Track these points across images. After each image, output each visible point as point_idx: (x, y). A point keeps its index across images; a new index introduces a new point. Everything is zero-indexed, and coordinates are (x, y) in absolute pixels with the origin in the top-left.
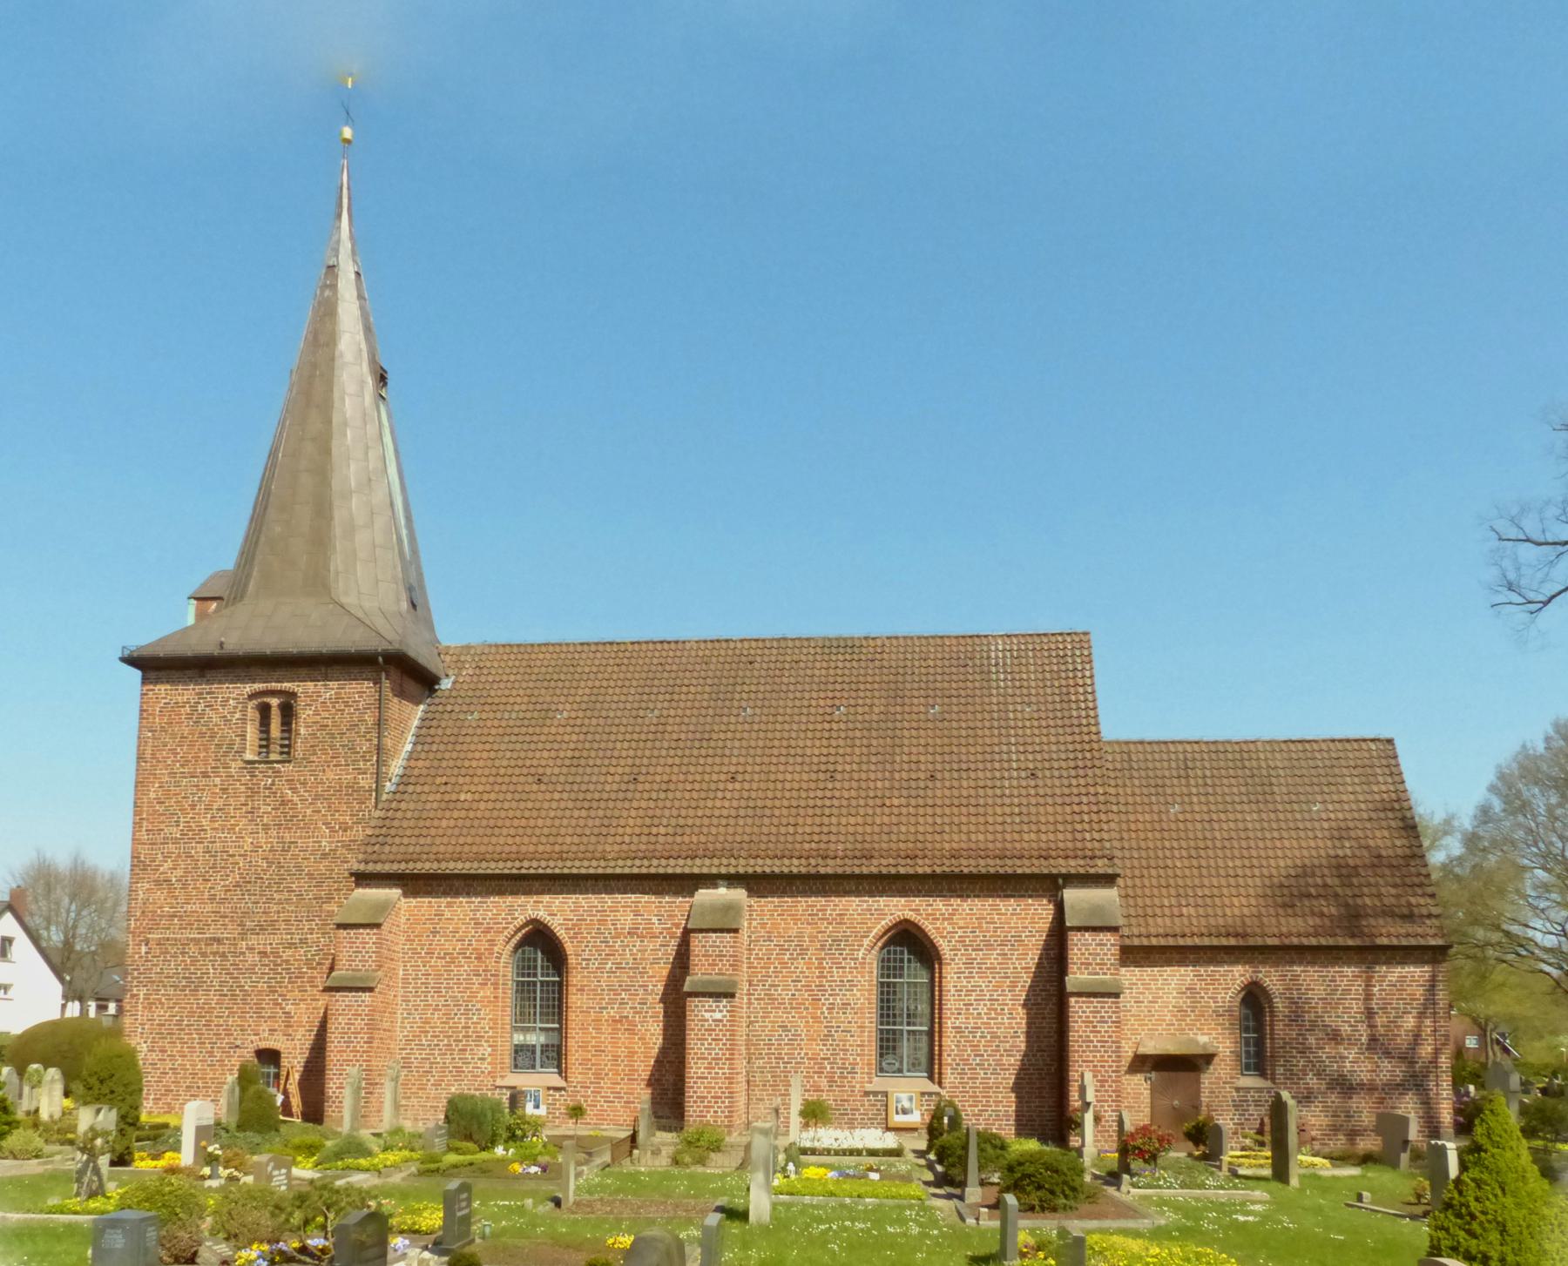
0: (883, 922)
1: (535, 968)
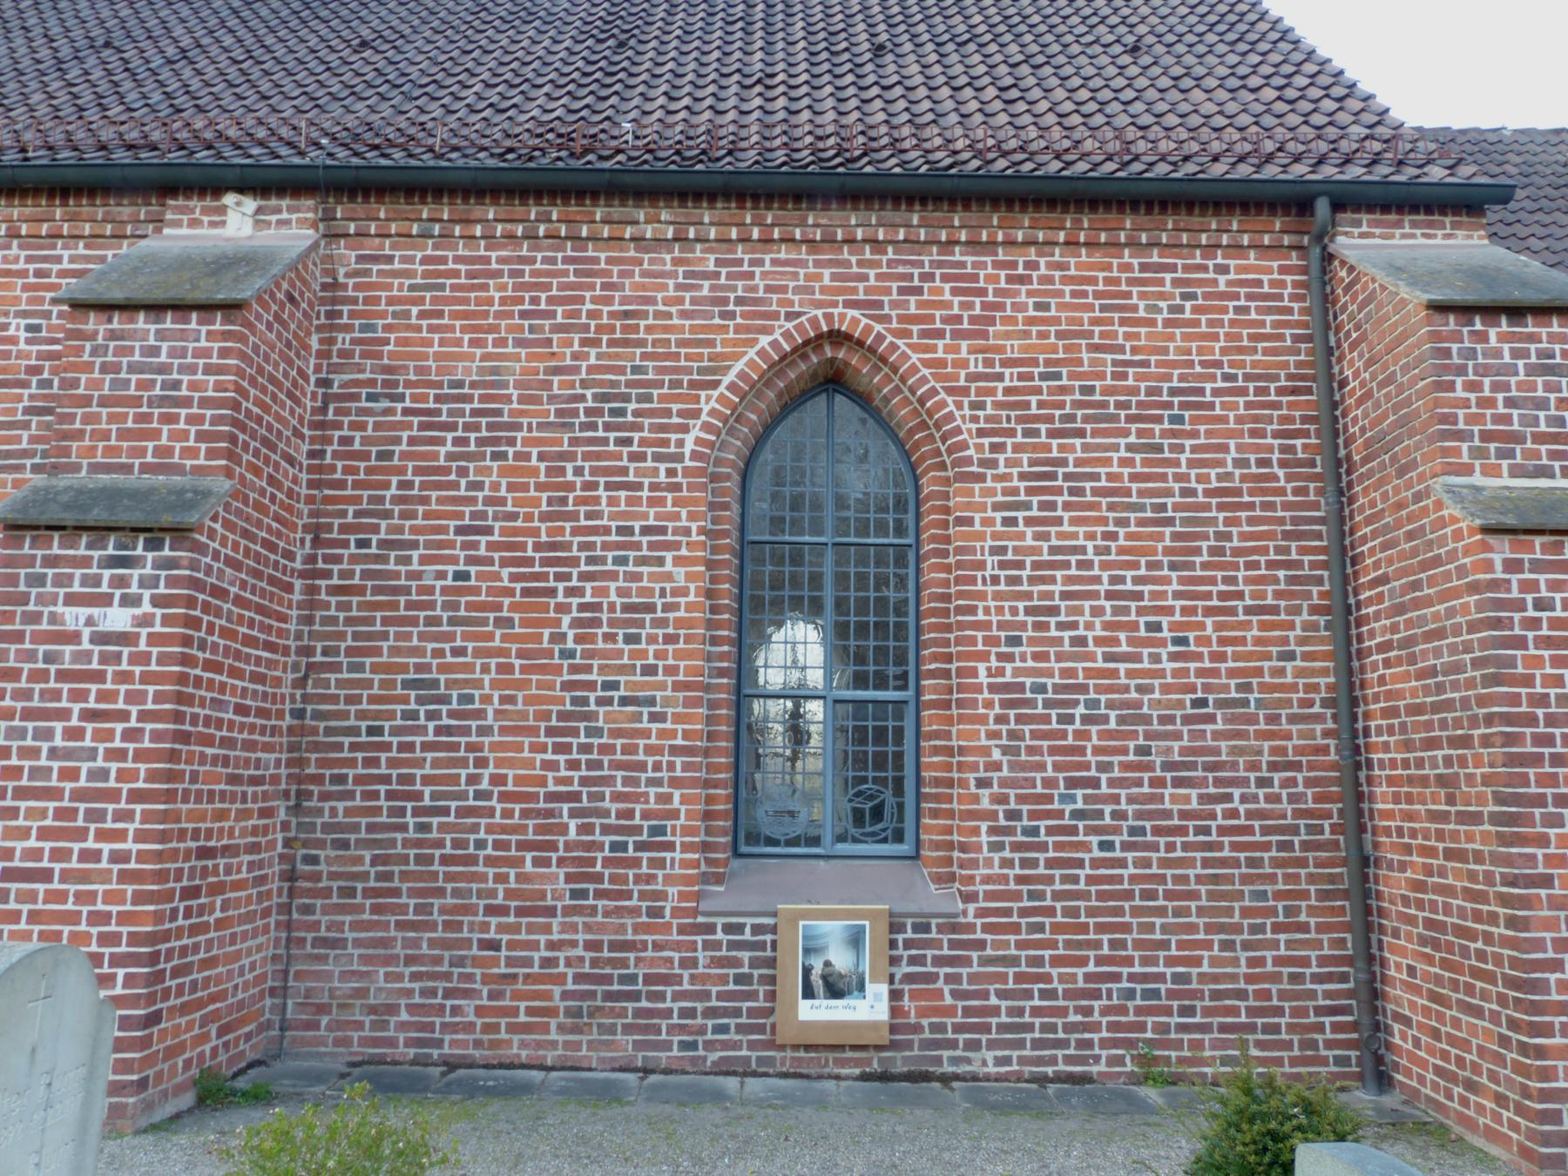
0: (764, 341)
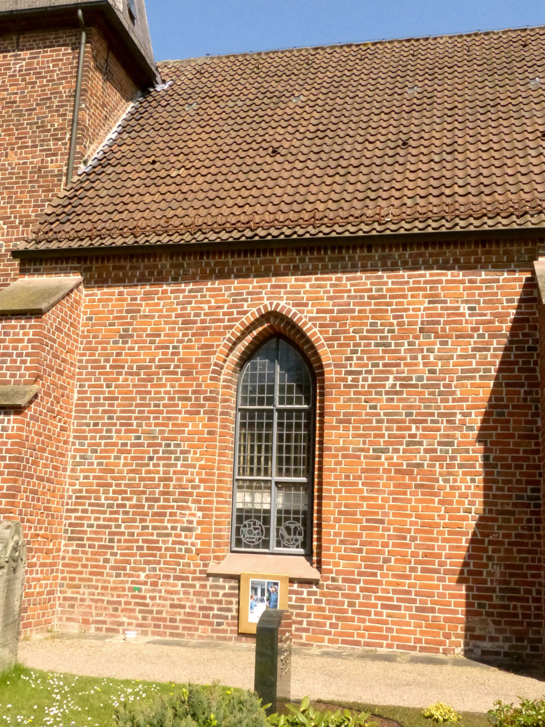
1: (271, 389)
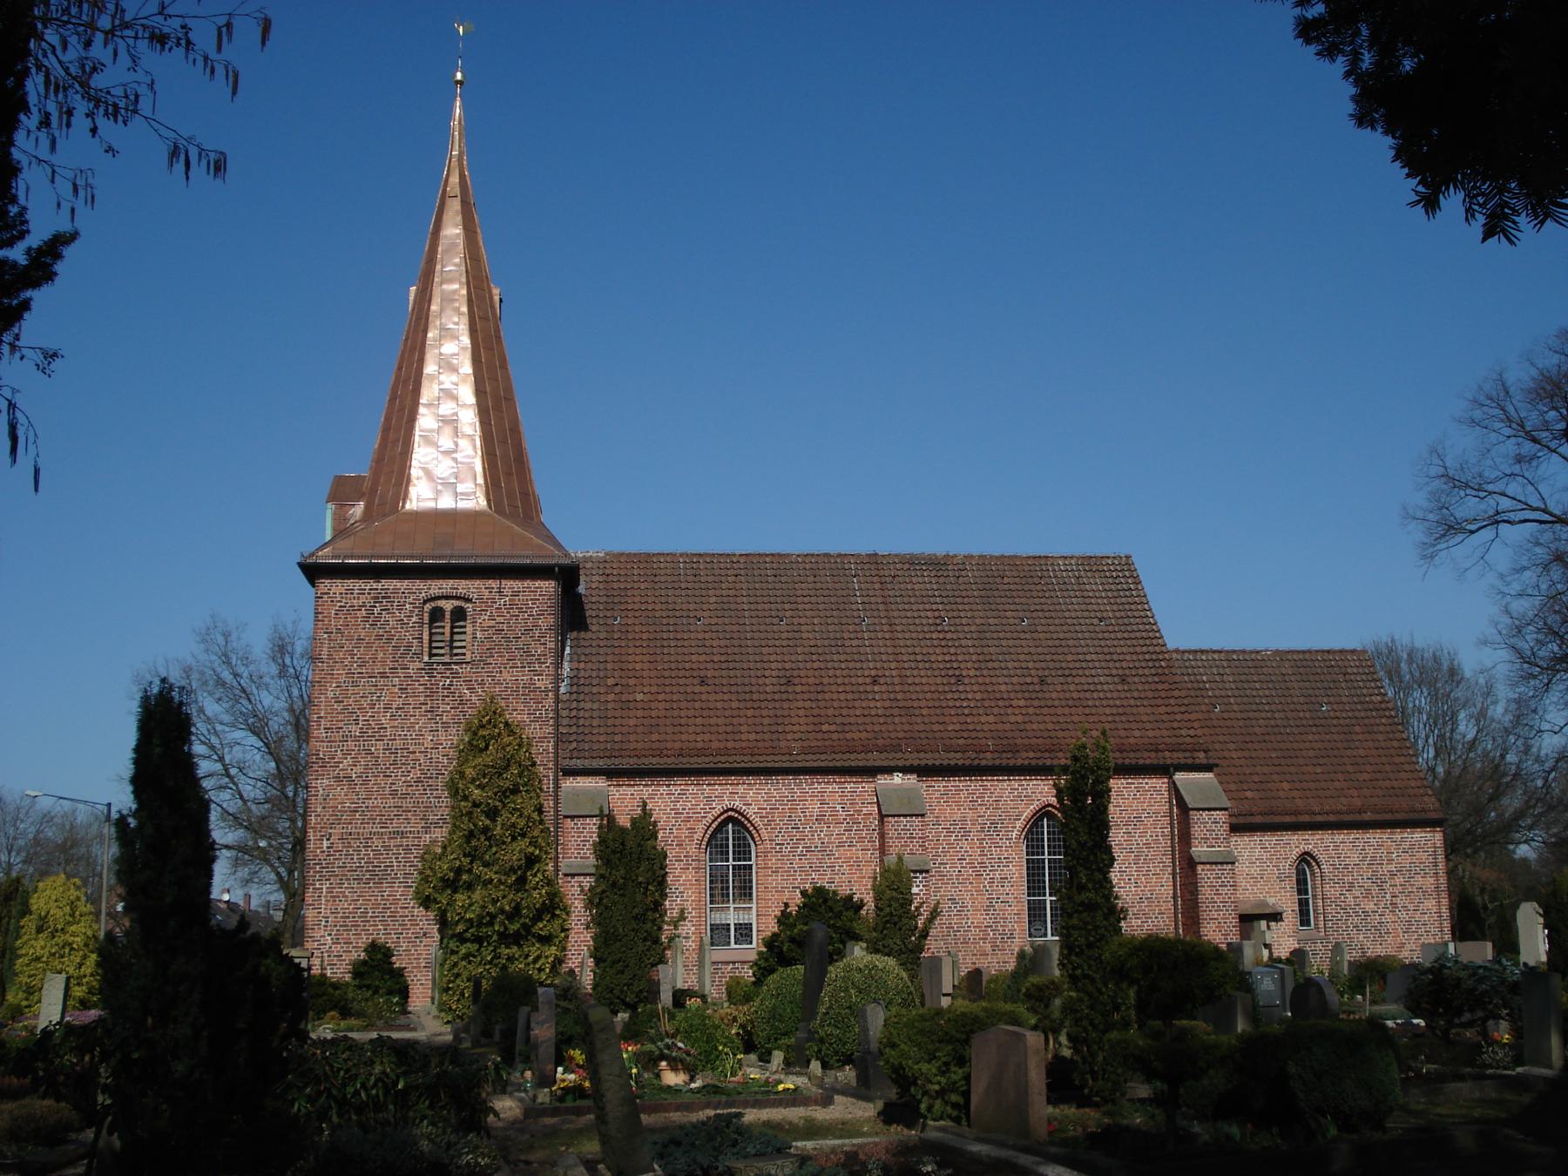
0: (1032, 807)
